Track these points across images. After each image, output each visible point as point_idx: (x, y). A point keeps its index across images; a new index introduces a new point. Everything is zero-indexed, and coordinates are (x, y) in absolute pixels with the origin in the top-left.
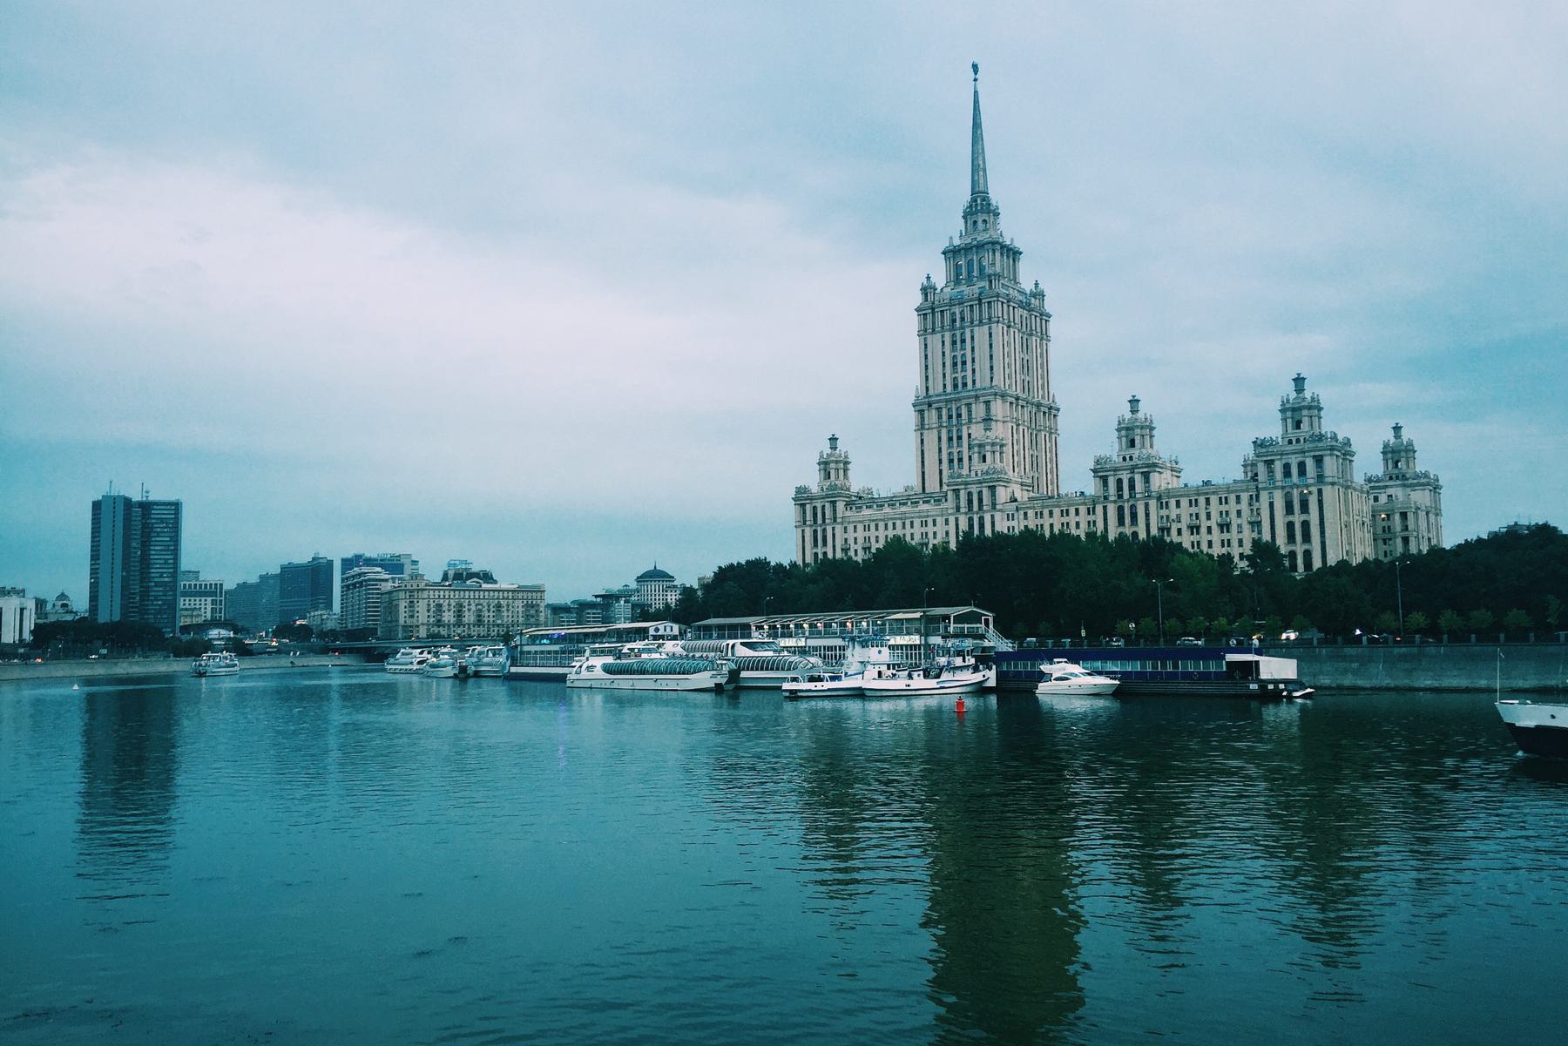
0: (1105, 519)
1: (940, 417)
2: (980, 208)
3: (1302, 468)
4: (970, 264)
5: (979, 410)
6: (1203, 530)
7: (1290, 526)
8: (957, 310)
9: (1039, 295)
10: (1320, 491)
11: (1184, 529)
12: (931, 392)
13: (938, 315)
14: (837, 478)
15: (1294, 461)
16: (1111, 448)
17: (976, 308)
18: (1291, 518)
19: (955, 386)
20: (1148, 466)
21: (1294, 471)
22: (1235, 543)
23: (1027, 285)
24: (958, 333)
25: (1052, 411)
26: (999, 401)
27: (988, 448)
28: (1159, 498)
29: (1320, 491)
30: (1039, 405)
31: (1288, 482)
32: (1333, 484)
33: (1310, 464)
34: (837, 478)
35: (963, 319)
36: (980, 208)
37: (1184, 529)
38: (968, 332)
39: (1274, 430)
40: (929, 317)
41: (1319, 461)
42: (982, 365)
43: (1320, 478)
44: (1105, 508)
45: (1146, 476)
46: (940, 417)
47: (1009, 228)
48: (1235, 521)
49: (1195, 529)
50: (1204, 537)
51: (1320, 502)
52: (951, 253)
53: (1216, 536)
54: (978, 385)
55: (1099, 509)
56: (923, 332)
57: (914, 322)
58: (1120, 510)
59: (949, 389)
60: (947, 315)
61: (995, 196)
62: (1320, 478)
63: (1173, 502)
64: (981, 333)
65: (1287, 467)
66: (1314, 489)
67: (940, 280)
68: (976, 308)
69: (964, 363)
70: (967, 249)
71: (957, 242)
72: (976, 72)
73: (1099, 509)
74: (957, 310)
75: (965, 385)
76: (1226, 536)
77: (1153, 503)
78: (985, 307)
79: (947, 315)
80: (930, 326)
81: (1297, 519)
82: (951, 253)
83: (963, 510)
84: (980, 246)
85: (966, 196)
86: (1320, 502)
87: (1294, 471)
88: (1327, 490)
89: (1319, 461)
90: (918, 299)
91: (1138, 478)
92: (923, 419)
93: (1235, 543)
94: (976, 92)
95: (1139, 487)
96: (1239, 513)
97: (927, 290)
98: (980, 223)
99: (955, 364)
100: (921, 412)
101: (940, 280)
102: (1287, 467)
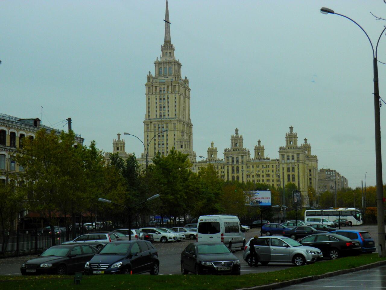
0: (228, 172)
1: (155, 127)
2: (168, 46)
3: (293, 156)
4: (165, 68)
5: (171, 126)
6: (261, 176)
7: (289, 176)
8: (162, 87)
9: (186, 81)
10: (298, 165)
11: (255, 175)
12: (151, 117)
13: (154, 88)
14: (121, 150)
15: (291, 155)
16: (229, 146)
17: (170, 87)
18: (289, 173)
19: (161, 116)
20: (243, 153)
21: (291, 158)
22: (271, 181)
23: (183, 78)
27: (183, 143)
28: (247, 164)
29: (298, 165)
31: (288, 161)
32: (302, 163)
33: (295, 156)
34: (121, 150)
35: (164, 91)
36: (168, 46)
37: (255, 175)
39: (284, 144)
41: (298, 155)
42: (172, 109)
43: (298, 161)
44: (228, 167)
45: (242, 156)
46: (155, 127)
47: (178, 55)
48: (271, 174)
49: (258, 175)
50: (261, 178)
51: (298, 169)
52: (157, 64)
53: (265, 178)
54: (170, 116)
55: (226, 167)
56: (148, 94)
57: (144, 90)
58: (233, 168)
59: (158, 117)
60: (158, 89)
61: (173, 43)
62: (298, 161)
63: (251, 166)
64: (172, 97)
65: (288, 156)
66: (296, 164)
67: (153, 74)
68: (170, 87)
69: (164, 107)
73: (226, 167)
74: (162, 87)
75: (164, 116)
76: (268, 178)
77: (245, 166)
78: (173, 87)
79: (158, 89)
80: (151, 91)
81: (291, 173)
82: (157, 64)
84: (170, 63)
85: (162, 43)
86: (298, 169)
87: (291, 158)
88: (301, 165)
89: (298, 155)
90: (146, 81)
91: (240, 157)
92: (148, 128)
93: (271, 181)
95: (240, 161)
96: (273, 171)
97: (149, 77)
98: (168, 53)
99: (160, 107)
100: (147, 125)
101: (153, 74)
102: (288, 156)
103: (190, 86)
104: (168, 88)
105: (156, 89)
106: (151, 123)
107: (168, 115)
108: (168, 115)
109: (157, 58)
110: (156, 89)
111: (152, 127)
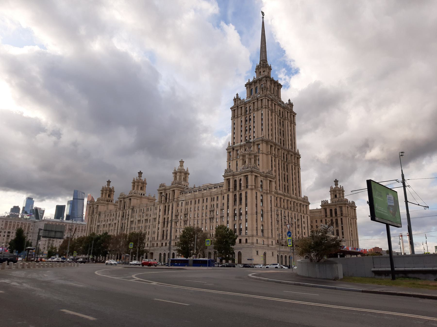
2: (263, 66)
13: (240, 109)
17: (256, 104)
24: (248, 116)
25: (297, 156)
26: (264, 145)
30: (288, 151)
38: (252, 114)
40: (236, 111)
57: (230, 113)
61: (269, 62)
64: (258, 115)
70: (255, 82)
71: (251, 80)
72: (263, 15)
78: (260, 102)
79: (243, 108)
83: (231, 190)
84: (260, 80)
90: (232, 104)
94: (263, 22)
100: (230, 153)
103: (294, 109)
104: (254, 105)
105: (241, 110)
106: (233, 149)
107: (254, 137)
108: (254, 137)
109: (249, 80)
110: (241, 110)
111: (234, 154)
